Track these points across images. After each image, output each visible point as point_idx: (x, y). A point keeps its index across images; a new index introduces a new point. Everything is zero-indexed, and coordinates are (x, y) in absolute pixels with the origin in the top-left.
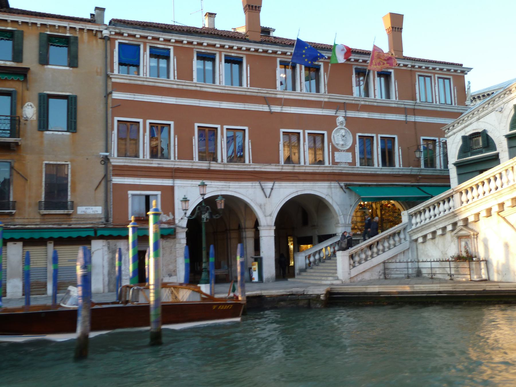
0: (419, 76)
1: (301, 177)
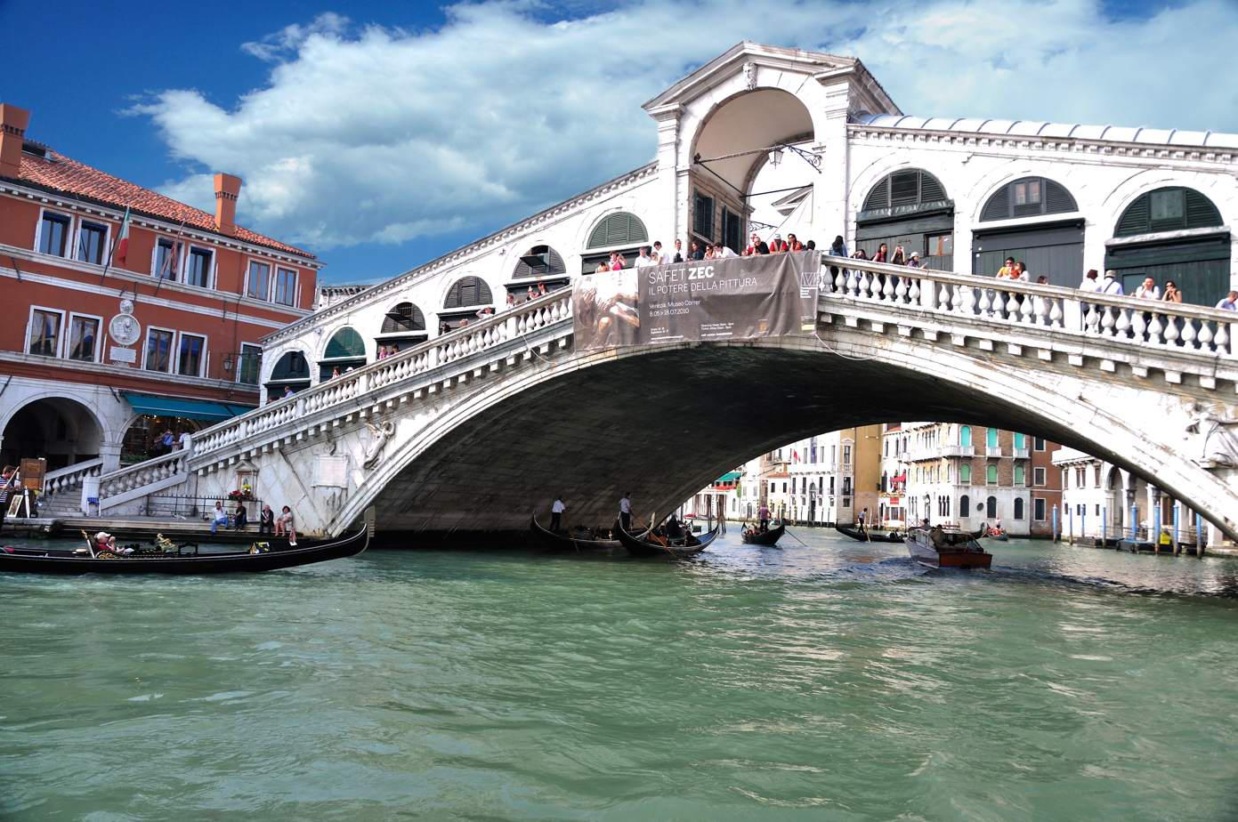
0: (252, 262)
1: (53, 373)
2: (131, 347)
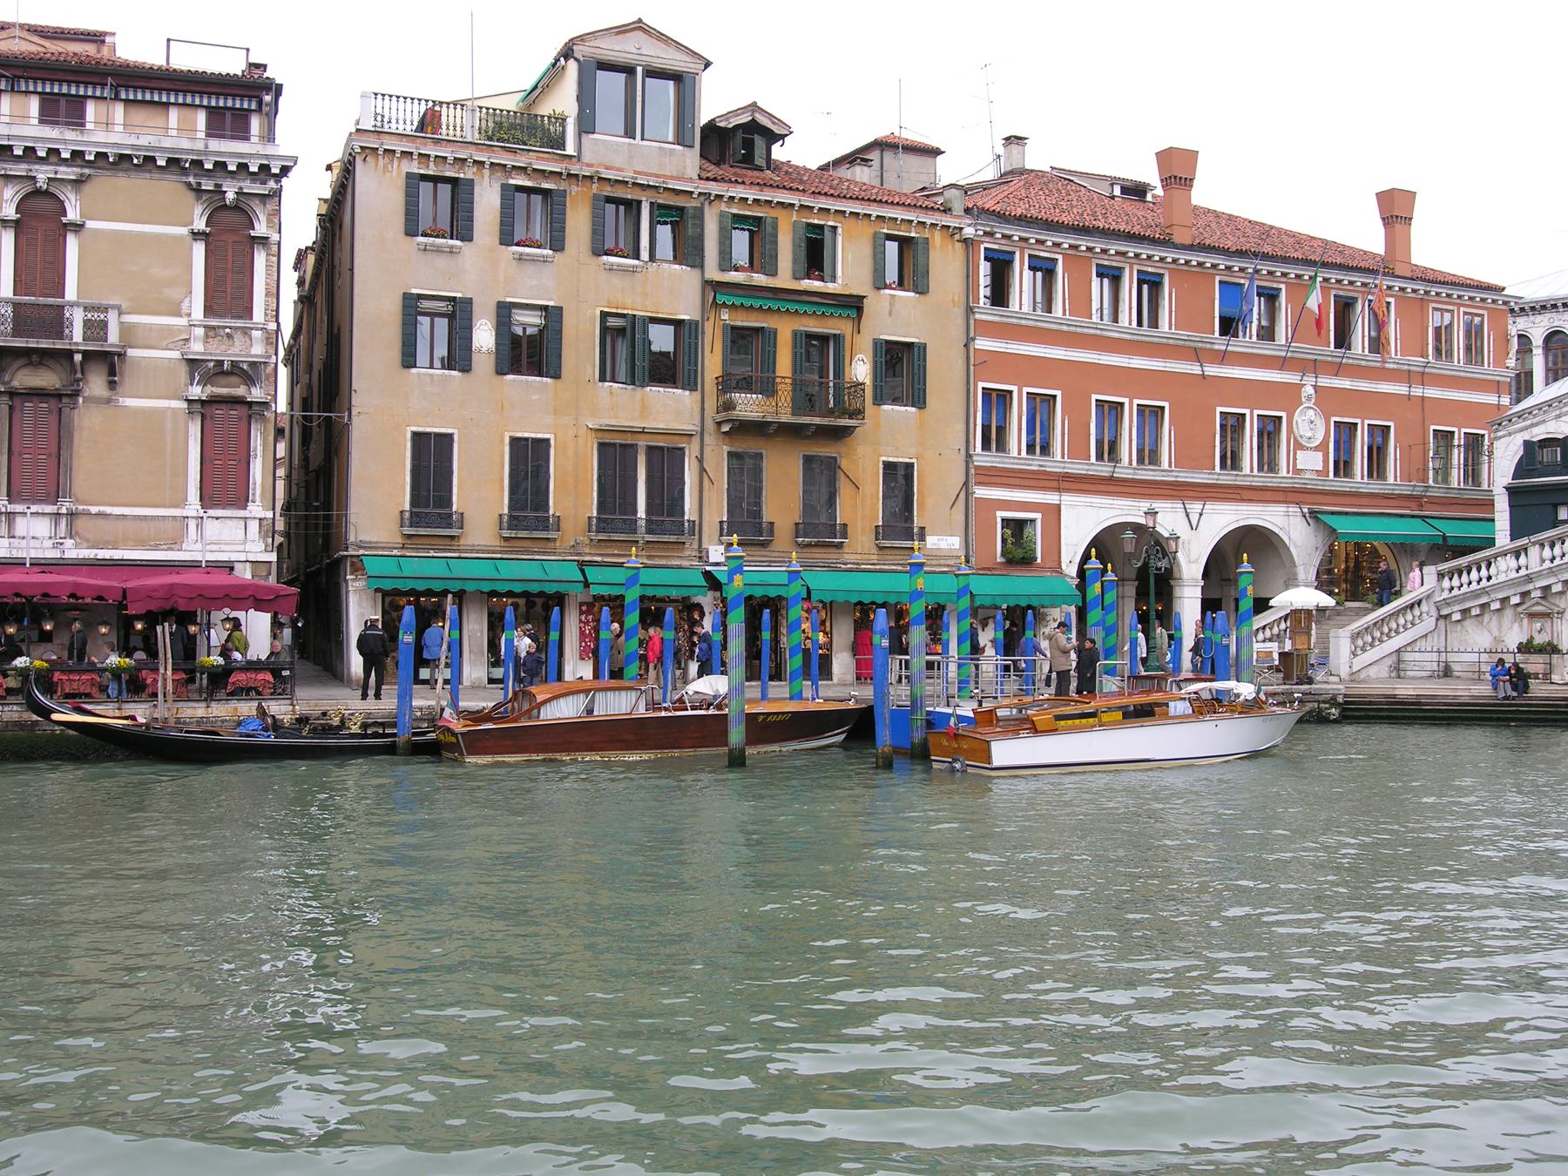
1: (1246, 494)
2: (1316, 449)
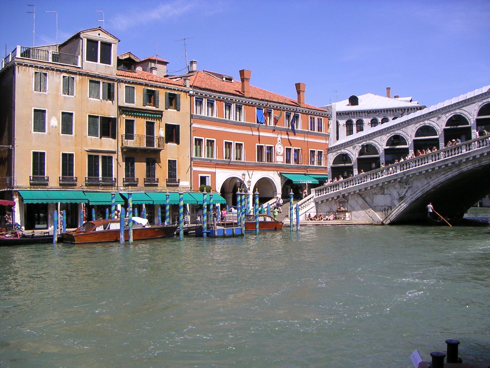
2: (281, 155)
